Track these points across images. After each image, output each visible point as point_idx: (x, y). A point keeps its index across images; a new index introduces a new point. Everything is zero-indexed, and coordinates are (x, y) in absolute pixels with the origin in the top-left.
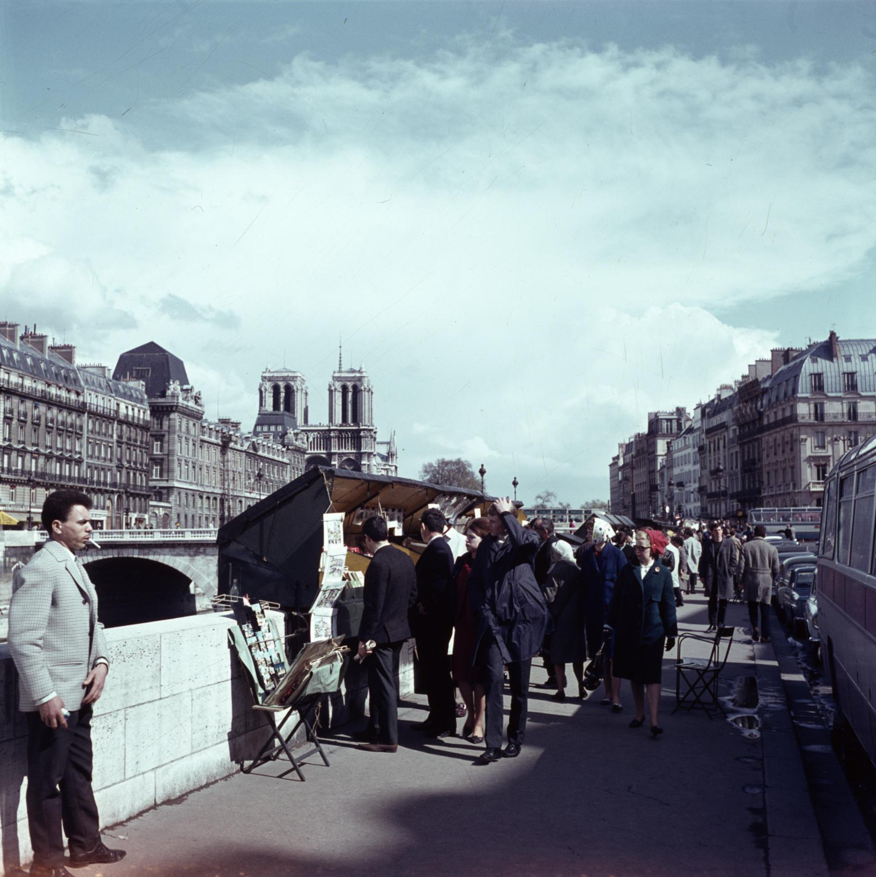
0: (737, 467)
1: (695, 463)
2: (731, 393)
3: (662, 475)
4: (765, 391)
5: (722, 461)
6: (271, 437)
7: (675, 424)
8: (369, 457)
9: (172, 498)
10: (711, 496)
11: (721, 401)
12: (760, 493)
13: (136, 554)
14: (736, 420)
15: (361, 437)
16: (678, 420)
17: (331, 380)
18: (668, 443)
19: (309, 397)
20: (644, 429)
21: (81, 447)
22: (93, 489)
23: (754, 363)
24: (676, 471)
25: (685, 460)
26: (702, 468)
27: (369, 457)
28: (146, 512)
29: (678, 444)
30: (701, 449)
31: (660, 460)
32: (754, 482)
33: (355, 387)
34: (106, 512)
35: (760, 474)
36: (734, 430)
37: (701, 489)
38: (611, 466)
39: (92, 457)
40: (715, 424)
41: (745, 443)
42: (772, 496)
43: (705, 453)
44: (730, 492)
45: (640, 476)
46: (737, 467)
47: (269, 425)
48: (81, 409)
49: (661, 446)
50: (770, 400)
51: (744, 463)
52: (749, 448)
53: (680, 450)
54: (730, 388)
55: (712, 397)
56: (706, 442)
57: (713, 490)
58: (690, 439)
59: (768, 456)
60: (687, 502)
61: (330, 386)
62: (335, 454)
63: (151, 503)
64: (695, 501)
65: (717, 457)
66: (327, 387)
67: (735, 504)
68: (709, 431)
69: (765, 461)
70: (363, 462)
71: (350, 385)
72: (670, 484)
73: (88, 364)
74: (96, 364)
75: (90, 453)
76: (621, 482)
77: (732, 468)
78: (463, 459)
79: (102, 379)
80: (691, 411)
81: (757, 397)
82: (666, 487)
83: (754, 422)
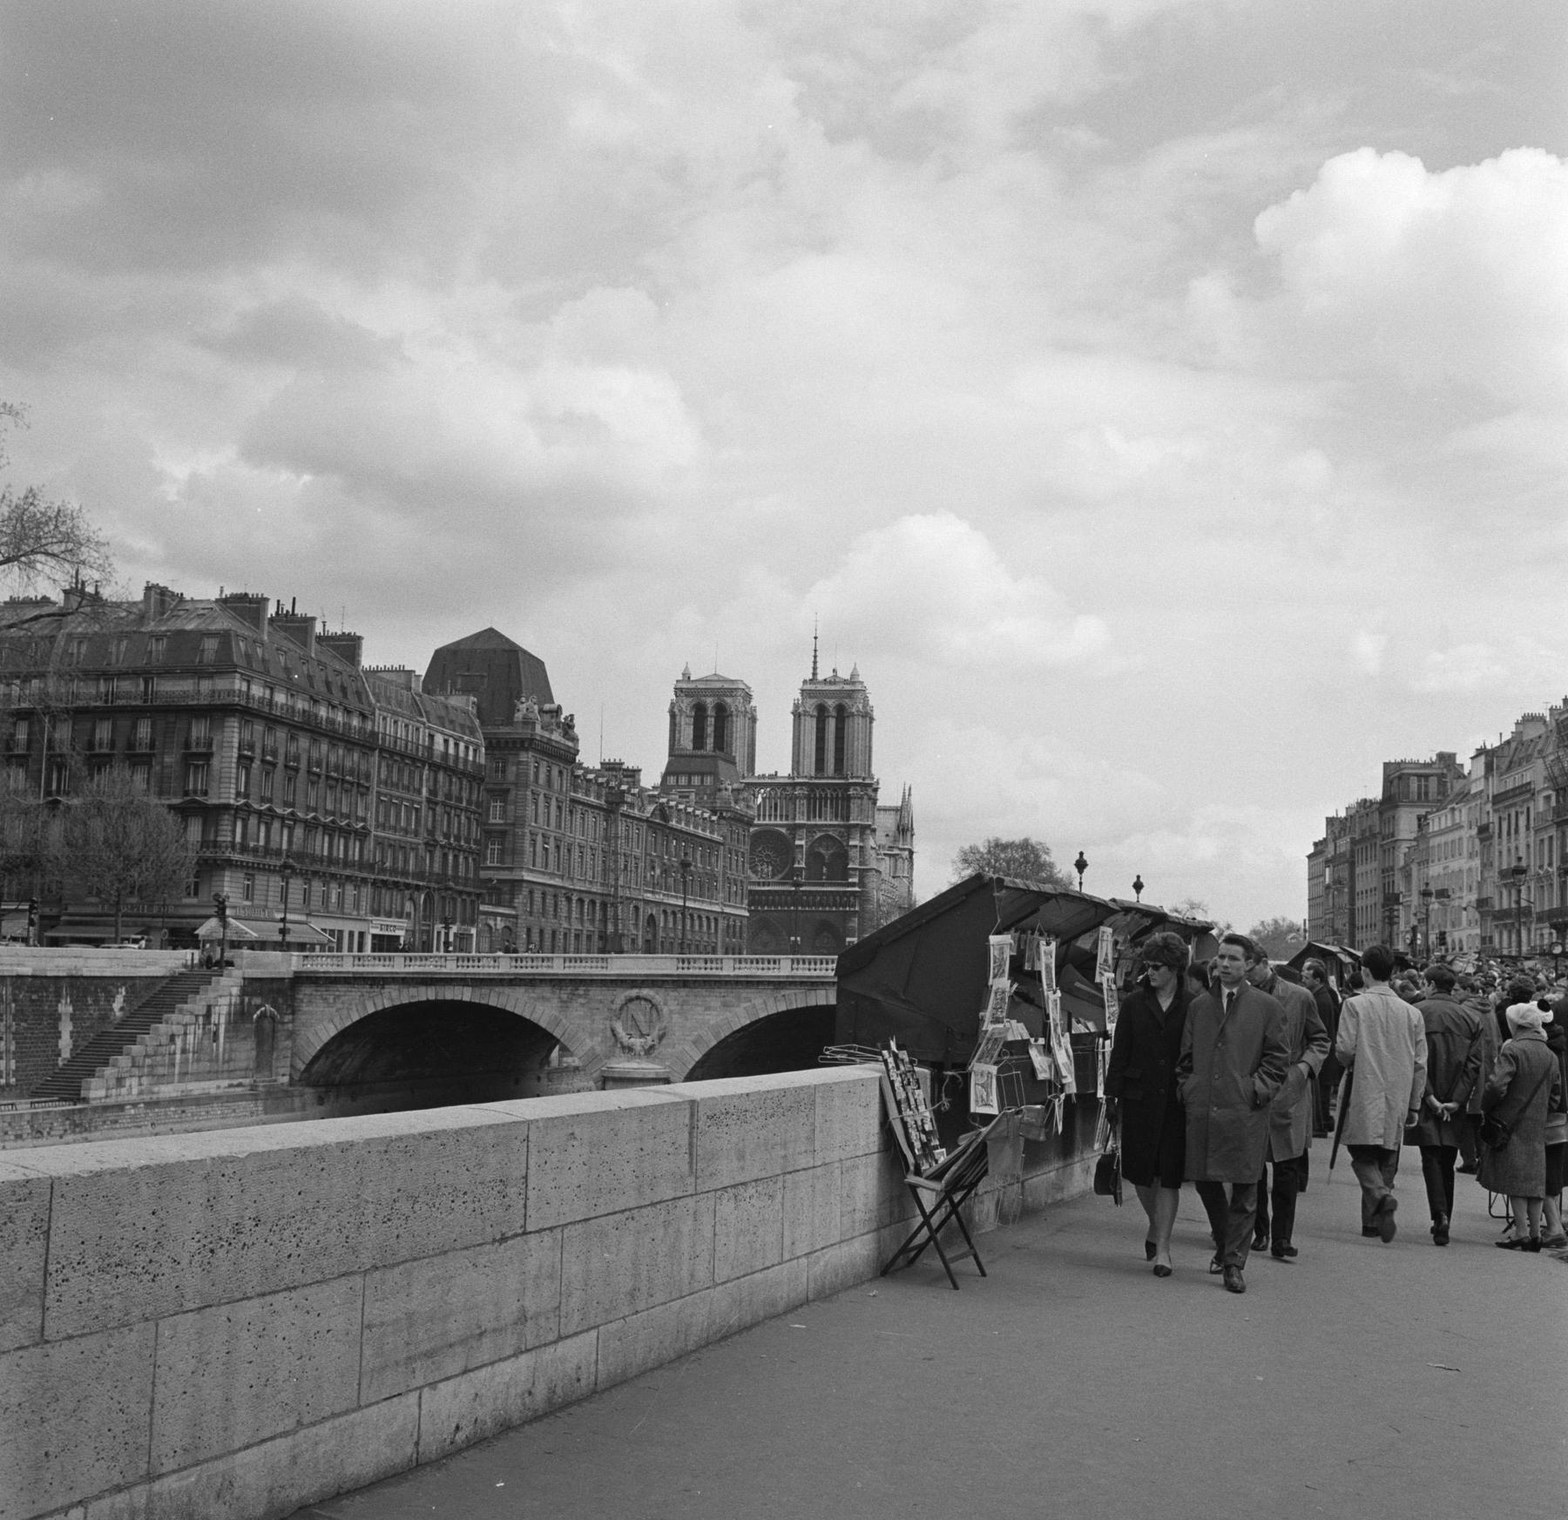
0: (1550, 865)
1: (1471, 856)
2: (1541, 730)
3: (1408, 877)
5: (1522, 853)
6: (693, 796)
7: (1433, 784)
8: (862, 834)
9: (519, 900)
10: (1501, 915)
13: (467, 994)
14: (1551, 779)
15: (849, 798)
16: (1441, 777)
18: (1419, 819)
20: (1376, 793)
21: (367, 811)
22: (384, 882)
24: (1435, 870)
25: (1453, 851)
26: (1486, 865)
27: (862, 834)
28: (473, 922)
29: (1437, 823)
30: (1483, 830)
31: (1403, 848)
33: (841, 709)
34: (404, 923)
36: (1548, 798)
37: (1482, 903)
38: (1309, 857)
39: (383, 827)
40: (1510, 786)
43: (1491, 837)
44: (1536, 909)
45: (1368, 875)
46: (1550, 865)
47: (690, 775)
48: (368, 744)
49: (1406, 824)
53: (1442, 833)
54: (1541, 719)
55: (1507, 737)
56: (1494, 818)
57: (1505, 906)
58: (1463, 814)
60: (1453, 925)
61: (796, 706)
62: (801, 826)
63: (483, 908)
64: (1470, 923)
65: (1513, 846)
67: (1546, 931)
68: (1497, 799)
70: (852, 843)
72: (1426, 894)
73: (381, 666)
74: (396, 666)
75: (381, 819)
76: (1328, 887)
77: (1541, 867)
78: (1033, 841)
79: (404, 692)
80: (1464, 759)
82: (1415, 899)
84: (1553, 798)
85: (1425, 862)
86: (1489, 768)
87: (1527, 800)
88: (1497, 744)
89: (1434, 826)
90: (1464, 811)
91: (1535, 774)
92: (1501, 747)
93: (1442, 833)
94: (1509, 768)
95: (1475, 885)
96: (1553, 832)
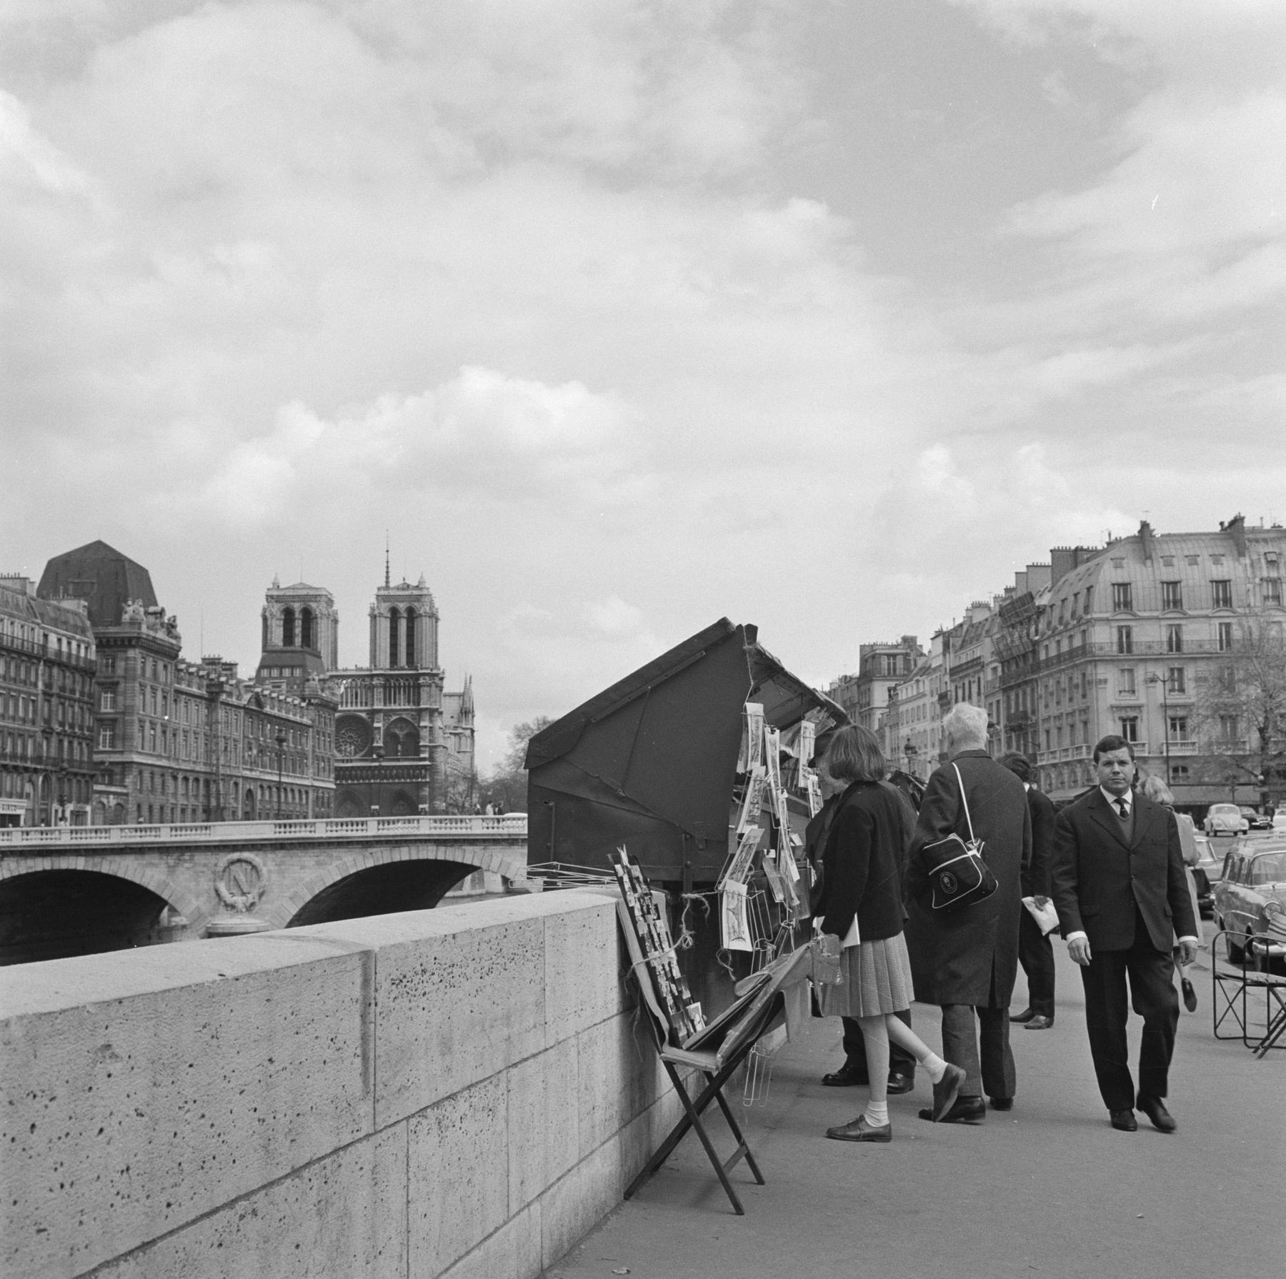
2: (987, 614)
4: (1041, 611)
7: (900, 662)
11: (972, 626)
12: (1035, 761)
17: (374, 600)
19: (340, 626)
20: (854, 670)
23: (1025, 570)
24: (904, 731)
29: (905, 693)
31: (878, 715)
32: (1025, 745)
33: (411, 611)
35: (1035, 733)
41: (1011, 688)
42: (1054, 765)
50: (1049, 623)
51: (1009, 718)
52: (1017, 695)
53: (908, 701)
59: (1046, 706)
66: (368, 611)
69: (1043, 712)
71: (402, 606)
81: (1029, 618)
83: (1024, 656)
84: (1000, 669)
85: (895, 726)
86: (946, 646)
87: (978, 672)
88: (951, 627)
89: (902, 696)
90: (927, 682)
91: (984, 650)
92: (955, 629)
93: (908, 701)
94: (962, 647)
95: (937, 743)
96: (1000, 696)
